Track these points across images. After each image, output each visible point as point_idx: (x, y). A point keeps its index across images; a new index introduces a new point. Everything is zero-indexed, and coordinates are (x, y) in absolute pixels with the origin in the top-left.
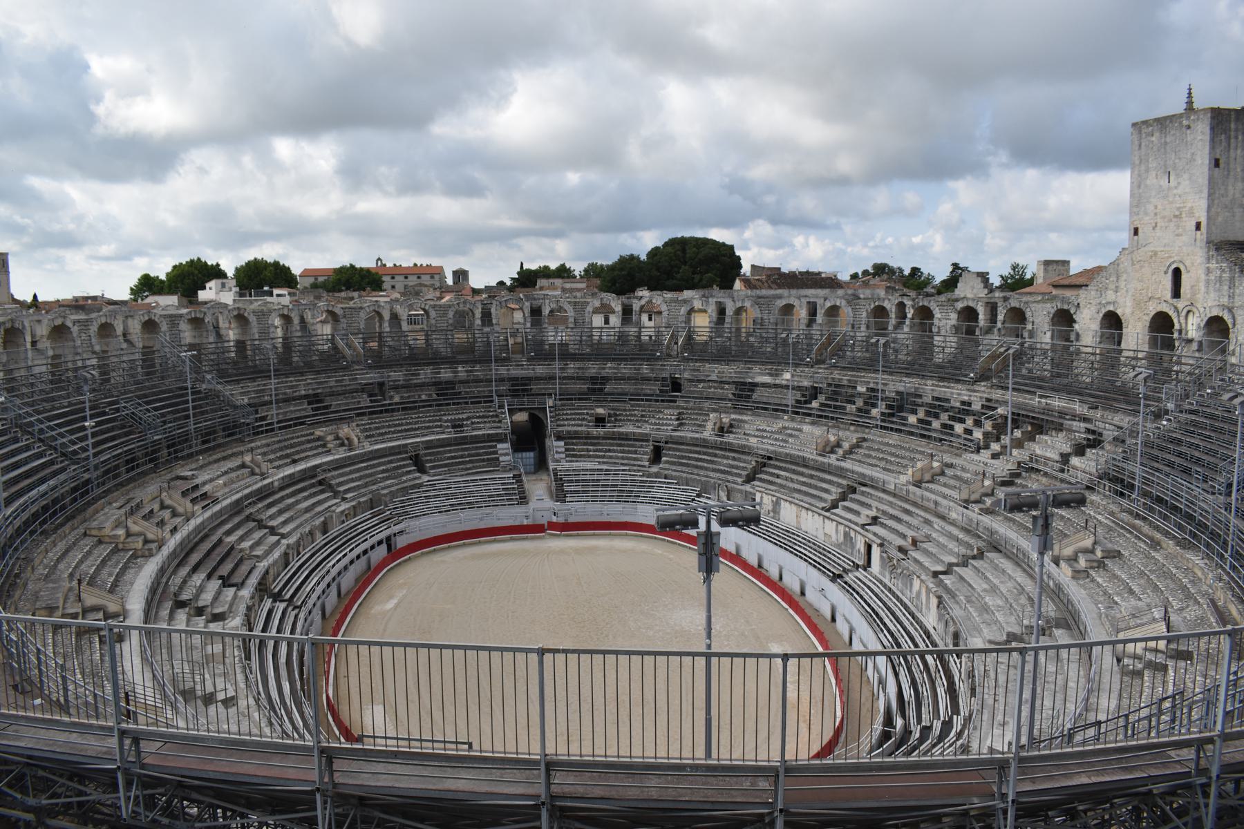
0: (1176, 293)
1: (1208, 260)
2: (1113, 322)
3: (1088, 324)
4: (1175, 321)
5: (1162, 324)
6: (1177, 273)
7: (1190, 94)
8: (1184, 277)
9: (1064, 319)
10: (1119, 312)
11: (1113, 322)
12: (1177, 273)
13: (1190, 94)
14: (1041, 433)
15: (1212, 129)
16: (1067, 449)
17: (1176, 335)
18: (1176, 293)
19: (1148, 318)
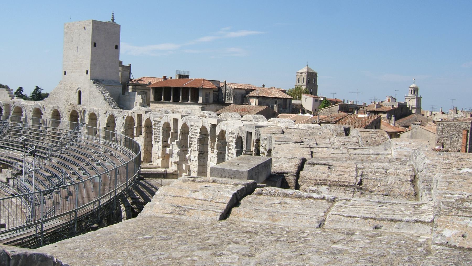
0: (80, 103)
1: (91, 87)
2: (56, 115)
3: (47, 116)
4: (79, 114)
5: (74, 116)
6: (80, 93)
7: (113, 16)
8: (82, 94)
9: (38, 113)
10: (59, 110)
11: (56, 115)
12: (80, 93)
13: (113, 16)
14: (5, 168)
15: (93, 29)
16: (10, 176)
17: (79, 122)
18: (80, 103)
19: (70, 113)
